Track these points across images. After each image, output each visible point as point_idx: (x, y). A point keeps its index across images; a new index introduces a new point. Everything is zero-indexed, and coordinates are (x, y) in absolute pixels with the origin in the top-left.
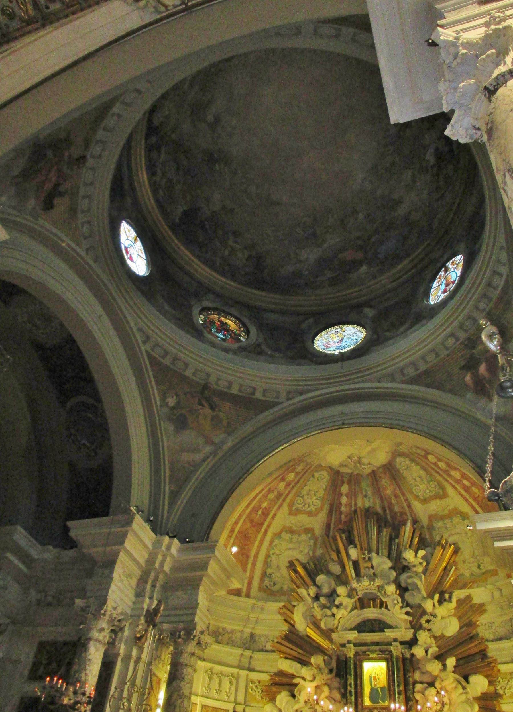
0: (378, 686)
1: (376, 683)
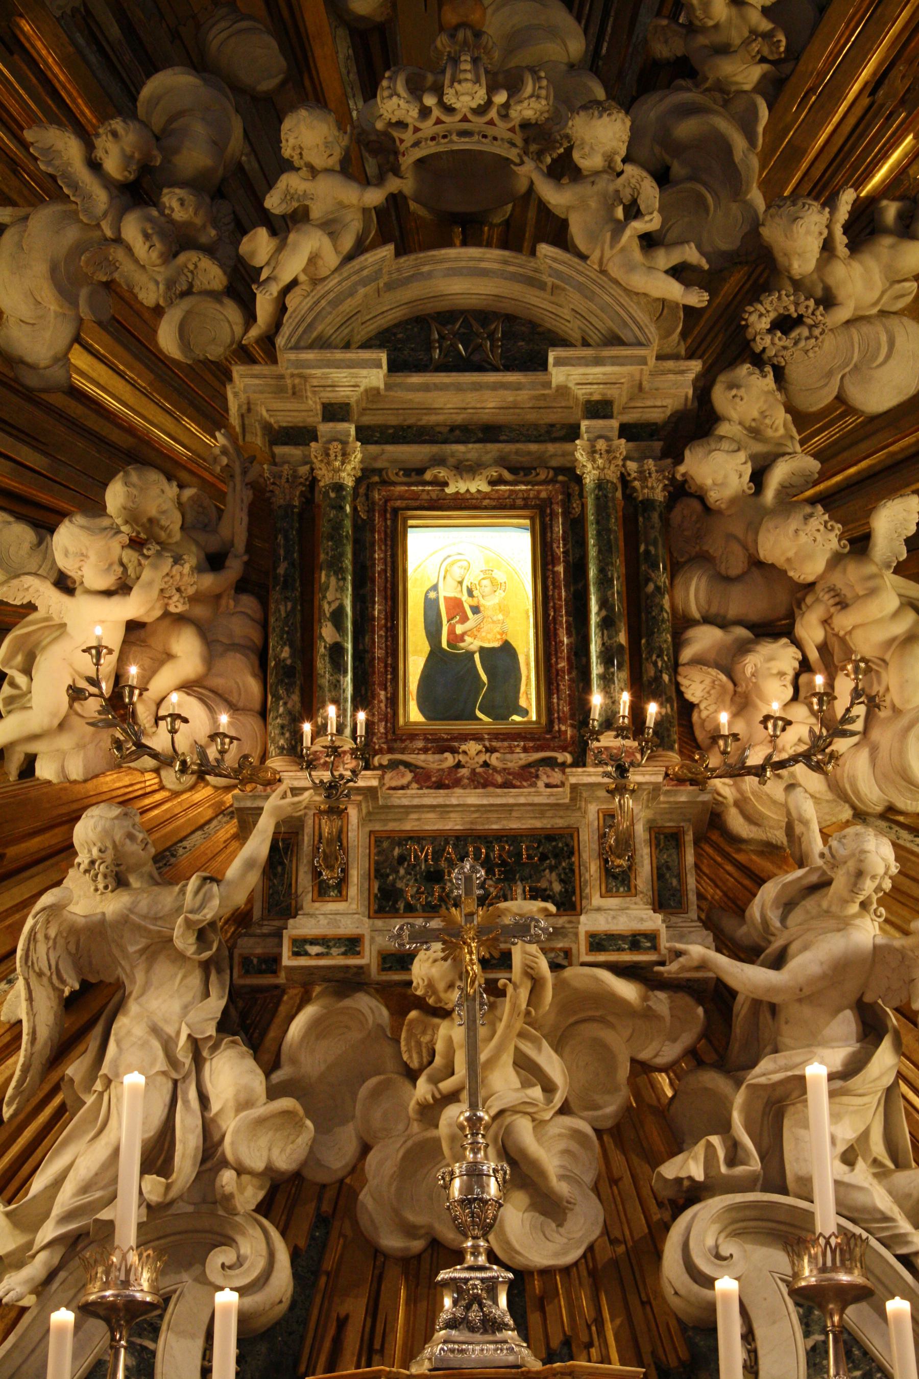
0: (472, 644)
1: (459, 629)
